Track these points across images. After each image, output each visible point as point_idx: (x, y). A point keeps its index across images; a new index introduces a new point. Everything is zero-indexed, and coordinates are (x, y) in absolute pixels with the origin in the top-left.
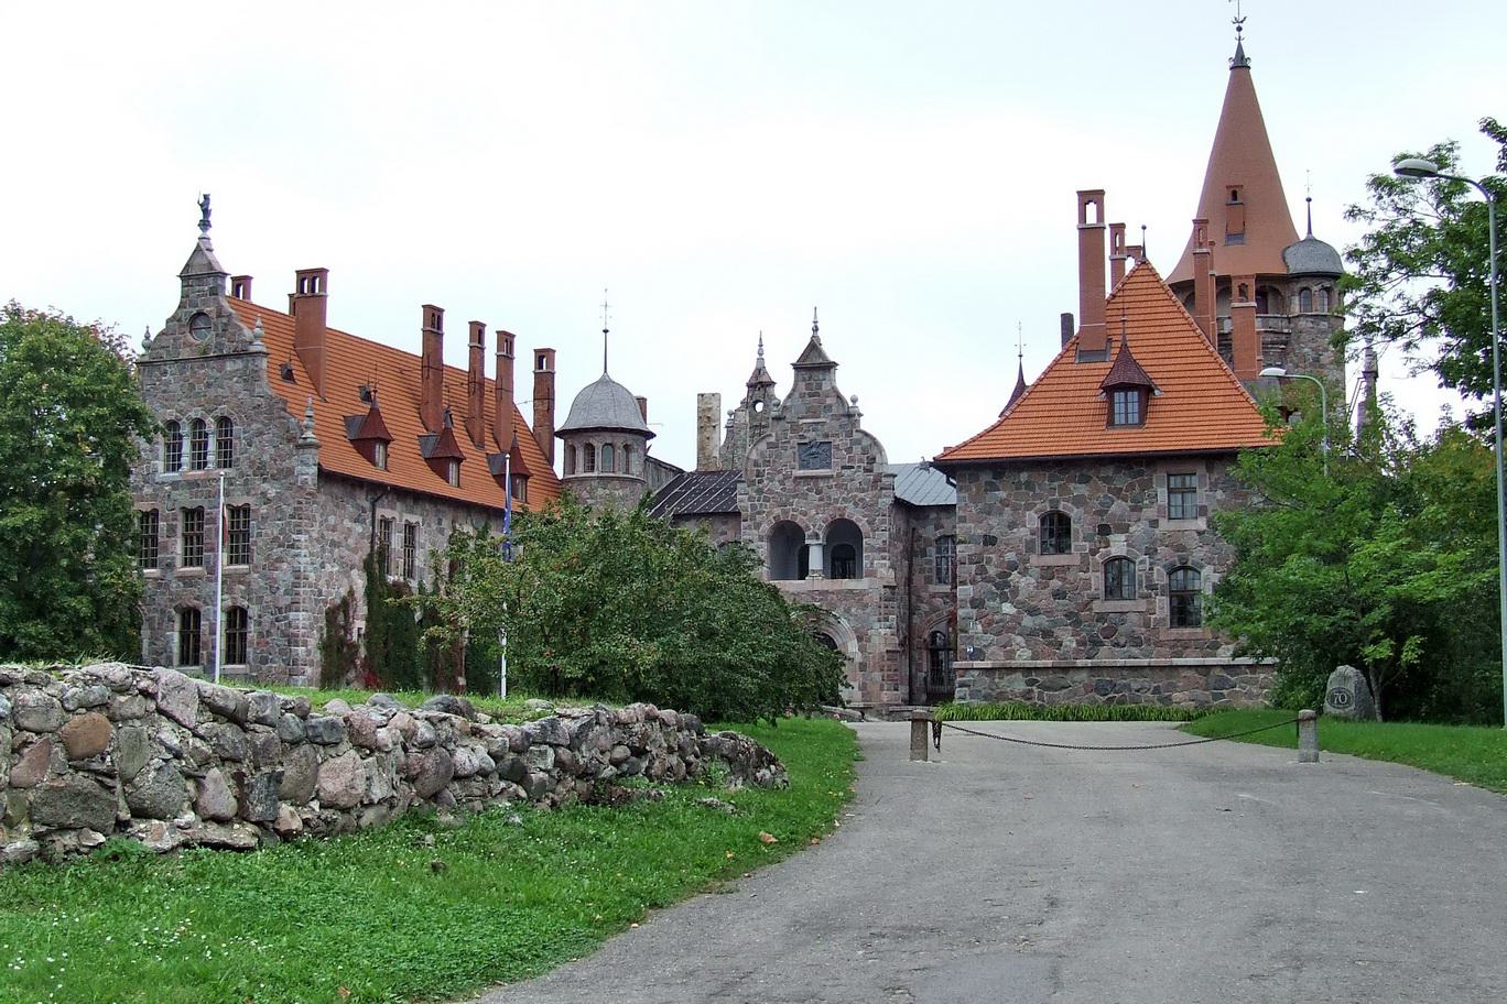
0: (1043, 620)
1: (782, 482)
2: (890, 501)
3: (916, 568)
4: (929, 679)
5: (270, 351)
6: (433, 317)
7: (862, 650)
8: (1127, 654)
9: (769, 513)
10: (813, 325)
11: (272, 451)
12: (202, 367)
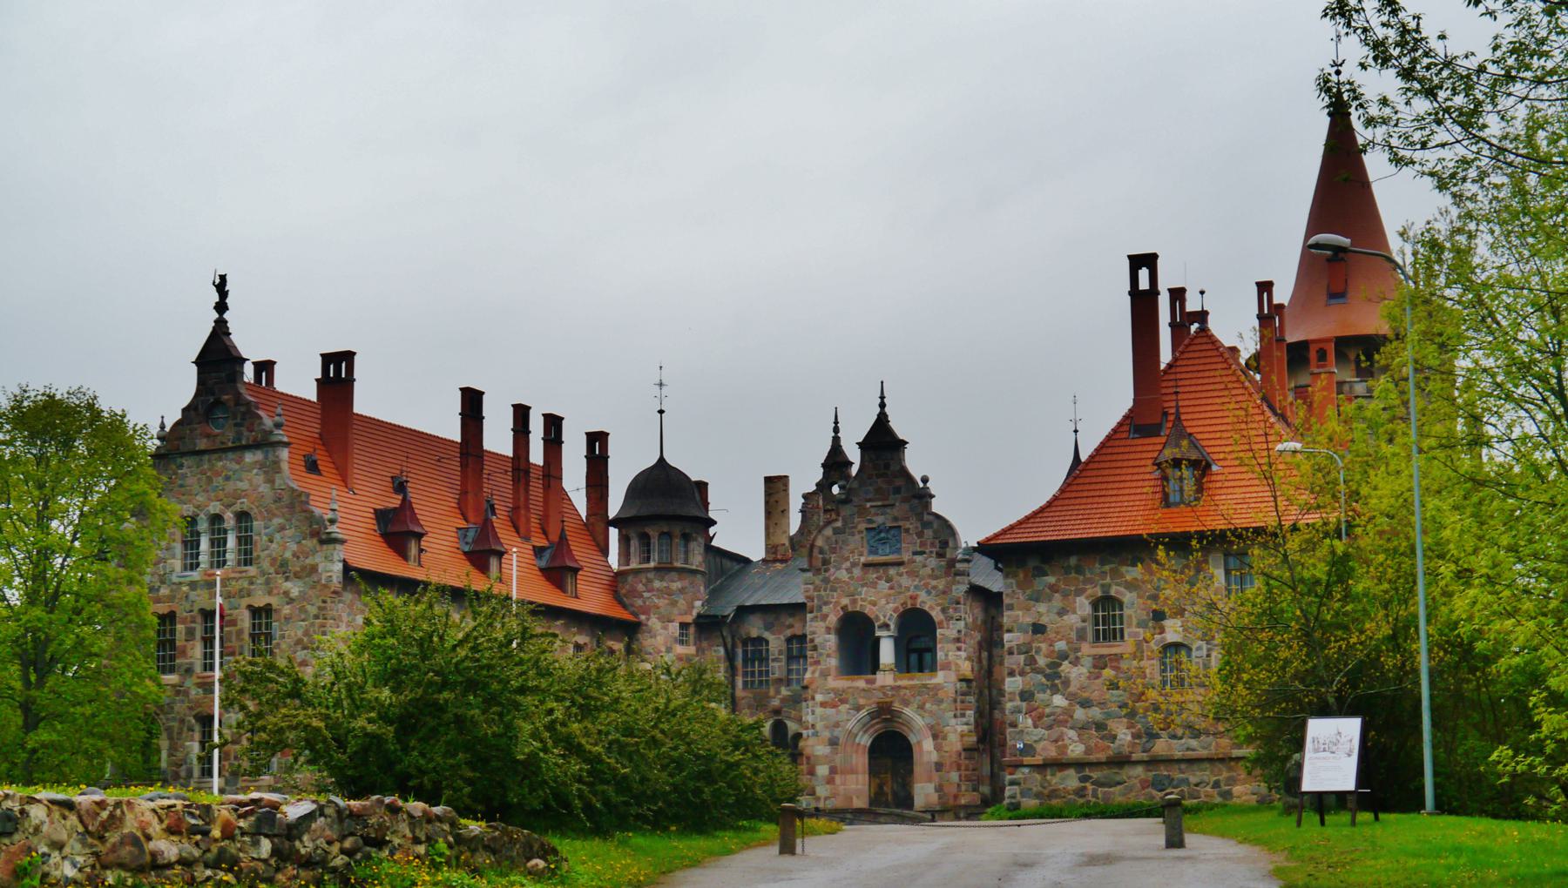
0: (1096, 713)
1: (849, 571)
2: (965, 587)
5: (292, 440)
6: (472, 402)
7: (938, 748)
8: (1186, 746)
9: (837, 603)
10: (879, 400)
11: (294, 547)
12: (220, 459)
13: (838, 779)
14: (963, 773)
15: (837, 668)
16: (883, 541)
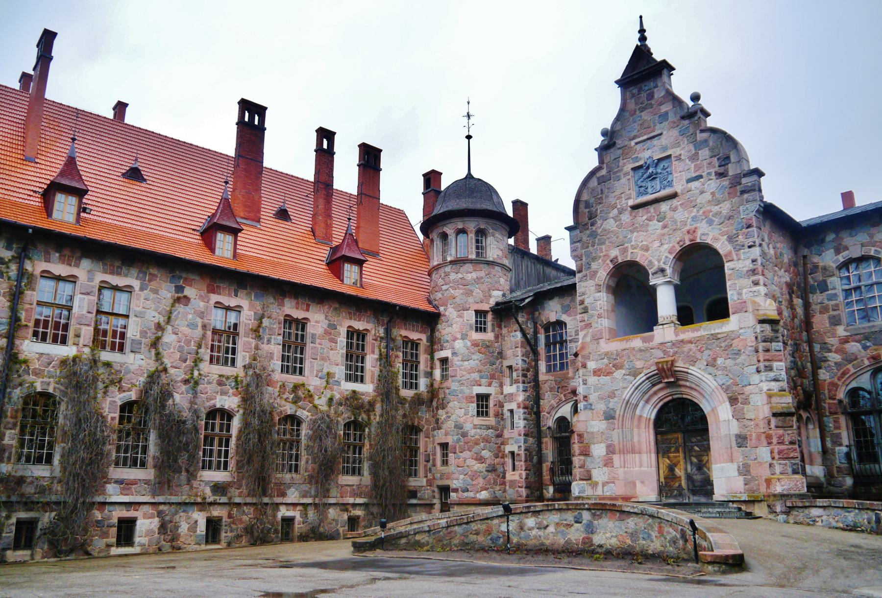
1: (616, 219)
2: (755, 206)
3: (816, 308)
4: (854, 456)
7: (738, 416)
13: (617, 459)
14: (776, 448)
15: (611, 330)
16: (652, 177)
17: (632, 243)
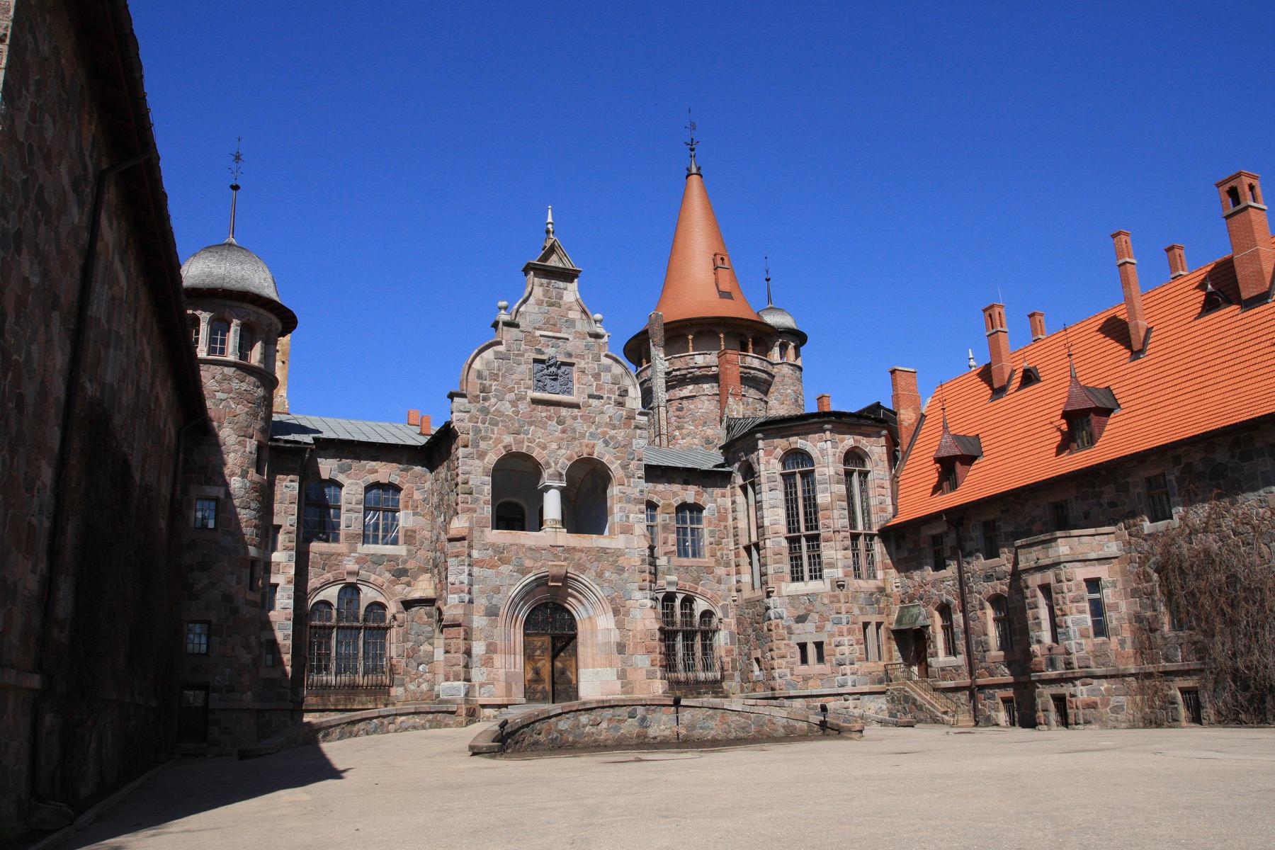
1: (514, 403)
7: (620, 626)
9: (499, 440)
13: (498, 659)
17: (529, 436)
